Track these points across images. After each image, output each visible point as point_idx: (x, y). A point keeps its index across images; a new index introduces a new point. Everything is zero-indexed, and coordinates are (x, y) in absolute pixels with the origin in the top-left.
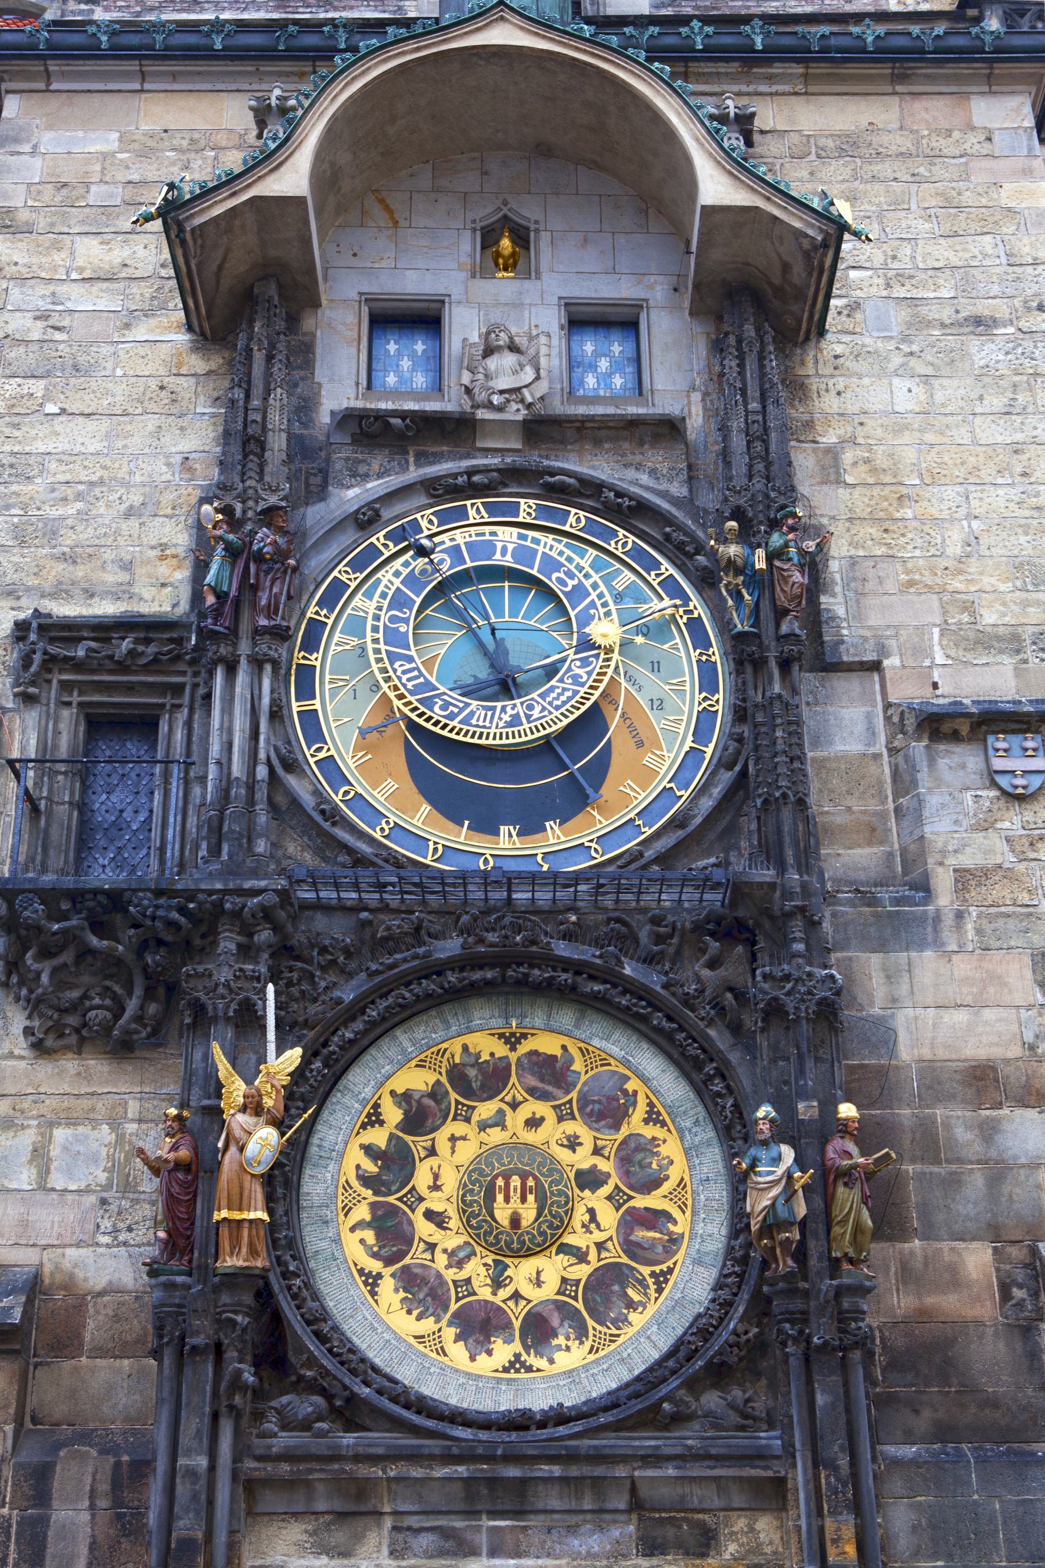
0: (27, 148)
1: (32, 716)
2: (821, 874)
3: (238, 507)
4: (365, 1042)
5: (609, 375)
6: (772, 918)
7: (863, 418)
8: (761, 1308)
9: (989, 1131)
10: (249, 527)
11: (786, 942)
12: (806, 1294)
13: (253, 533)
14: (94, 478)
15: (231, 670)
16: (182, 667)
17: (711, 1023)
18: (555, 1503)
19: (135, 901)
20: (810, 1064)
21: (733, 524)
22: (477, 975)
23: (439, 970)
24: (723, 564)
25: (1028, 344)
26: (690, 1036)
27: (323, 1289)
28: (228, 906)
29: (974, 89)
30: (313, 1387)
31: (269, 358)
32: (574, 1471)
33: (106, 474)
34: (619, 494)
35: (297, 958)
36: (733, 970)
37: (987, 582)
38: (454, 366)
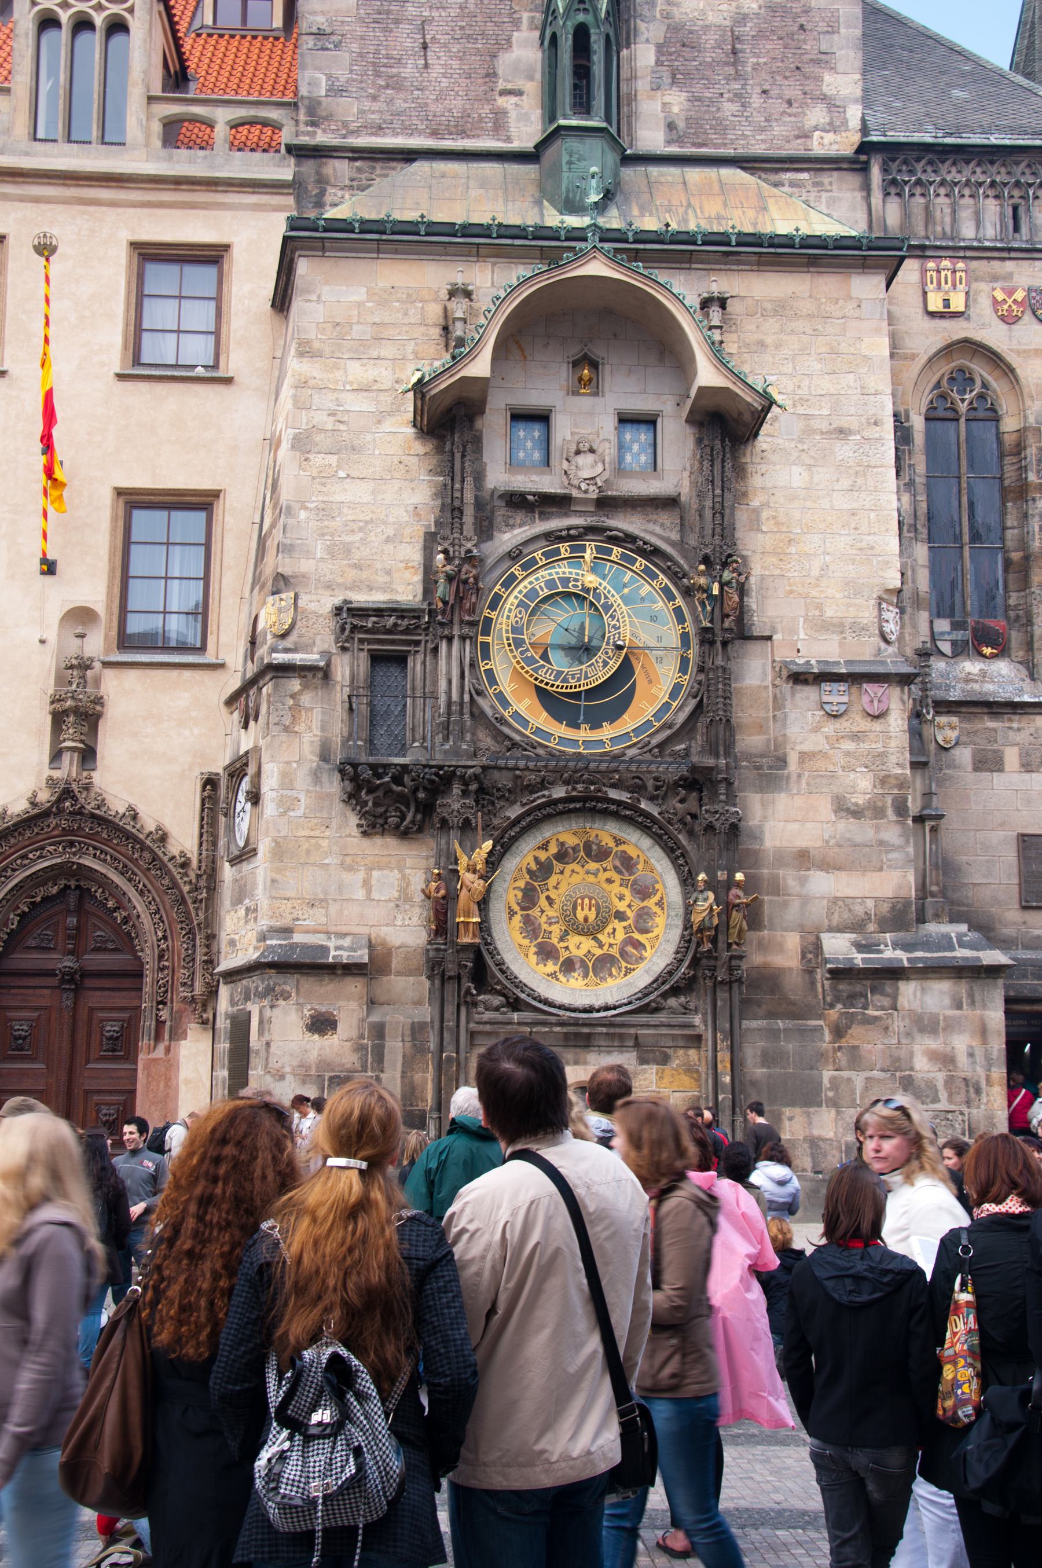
0: (314, 297)
1: (346, 657)
2: (736, 757)
3: (451, 550)
5: (639, 454)
6: (711, 781)
7: (774, 491)
8: (695, 962)
9: (803, 881)
11: (717, 794)
12: (716, 958)
14: (368, 518)
18: (603, 1043)
20: (725, 854)
21: (702, 567)
22: (572, 806)
23: (555, 802)
25: (866, 447)
27: (500, 945)
31: (463, 456)
32: (612, 1030)
33: (374, 516)
34: (645, 543)
36: (692, 804)
37: (830, 592)
38: (558, 454)
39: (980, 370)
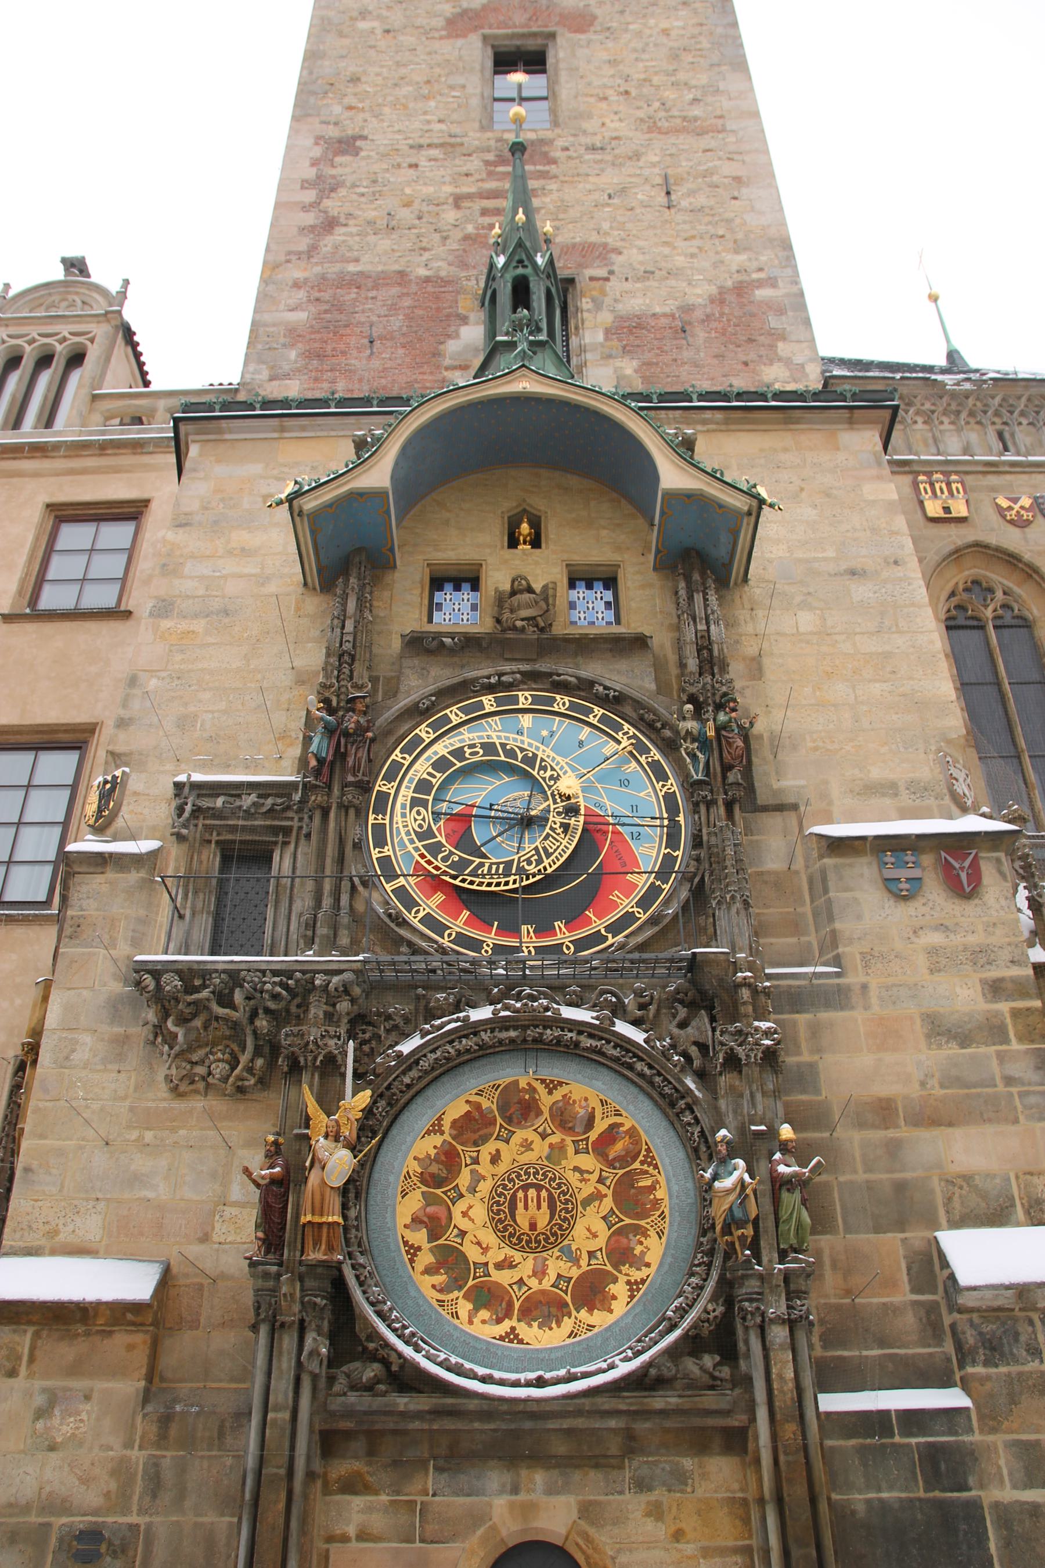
4: (421, 1085)
8: (726, 1291)
9: (893, 1148)
10: (341, 713)
13: (344, 716)
15: (325, 812)
16: (290, 814)
17: (682, 1070)
19: (248, 978)
22: (504, 1035)
23: (473, 1029)
24: (683, 733)
26: (665, 1079)
28: (317, 982)
29: (840, 426)
30: (373, 1357)
34: (606, 688)
35: (369, 1024)
39: (999, 578)
